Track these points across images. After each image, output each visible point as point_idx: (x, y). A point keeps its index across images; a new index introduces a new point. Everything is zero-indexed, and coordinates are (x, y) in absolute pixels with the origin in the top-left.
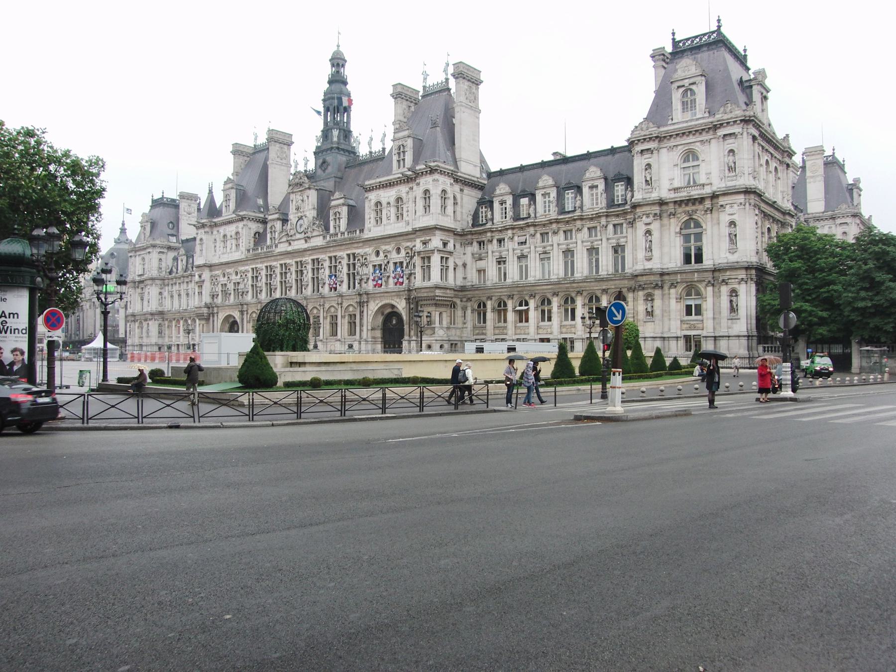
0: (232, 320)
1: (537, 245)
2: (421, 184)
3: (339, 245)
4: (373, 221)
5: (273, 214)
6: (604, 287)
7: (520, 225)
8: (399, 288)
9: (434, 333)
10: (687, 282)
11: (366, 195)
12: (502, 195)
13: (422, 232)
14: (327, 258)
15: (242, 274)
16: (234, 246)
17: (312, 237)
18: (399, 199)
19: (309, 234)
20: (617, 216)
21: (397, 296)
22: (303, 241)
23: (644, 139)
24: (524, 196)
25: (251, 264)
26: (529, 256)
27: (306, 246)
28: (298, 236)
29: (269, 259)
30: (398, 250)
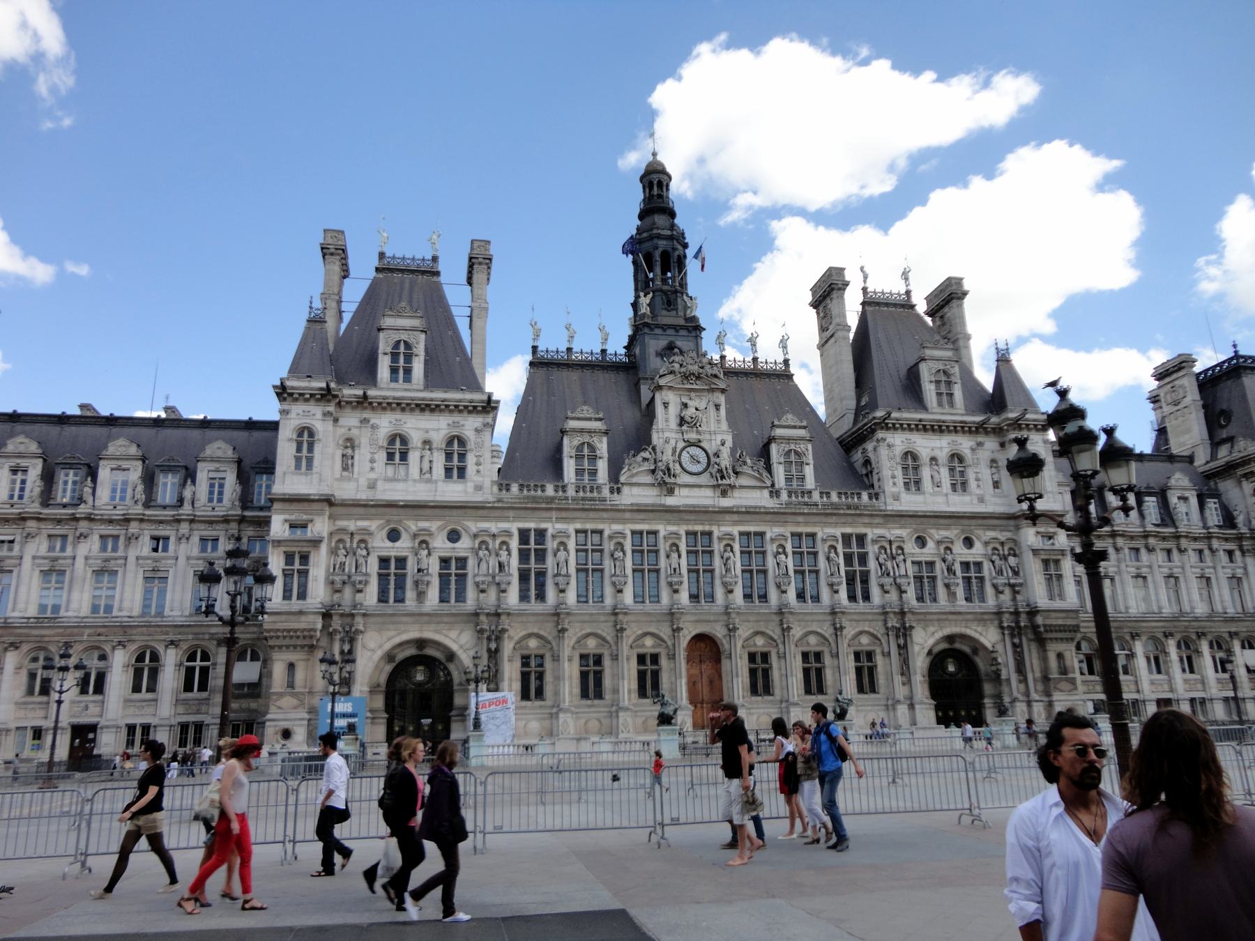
0: (411, 651)
3: (821, 514)
4: (900, 480)
5: (590, 419)
6: (1233, 630)
8: (980, 607)
9: (1076, 688)
14: (789, 535)
15: (490, 541)
16: (439, 470)
17: (742, 487)
18: (956, 457)
19: (732, 480)
20: (1226, 540)
21: (980, 620)
22: (709, 492)
25: (515, 519)
26: (1117, 578)
27: (726, 502)
28: (685, 479)
29: (592, 514)
30: (969, 542)
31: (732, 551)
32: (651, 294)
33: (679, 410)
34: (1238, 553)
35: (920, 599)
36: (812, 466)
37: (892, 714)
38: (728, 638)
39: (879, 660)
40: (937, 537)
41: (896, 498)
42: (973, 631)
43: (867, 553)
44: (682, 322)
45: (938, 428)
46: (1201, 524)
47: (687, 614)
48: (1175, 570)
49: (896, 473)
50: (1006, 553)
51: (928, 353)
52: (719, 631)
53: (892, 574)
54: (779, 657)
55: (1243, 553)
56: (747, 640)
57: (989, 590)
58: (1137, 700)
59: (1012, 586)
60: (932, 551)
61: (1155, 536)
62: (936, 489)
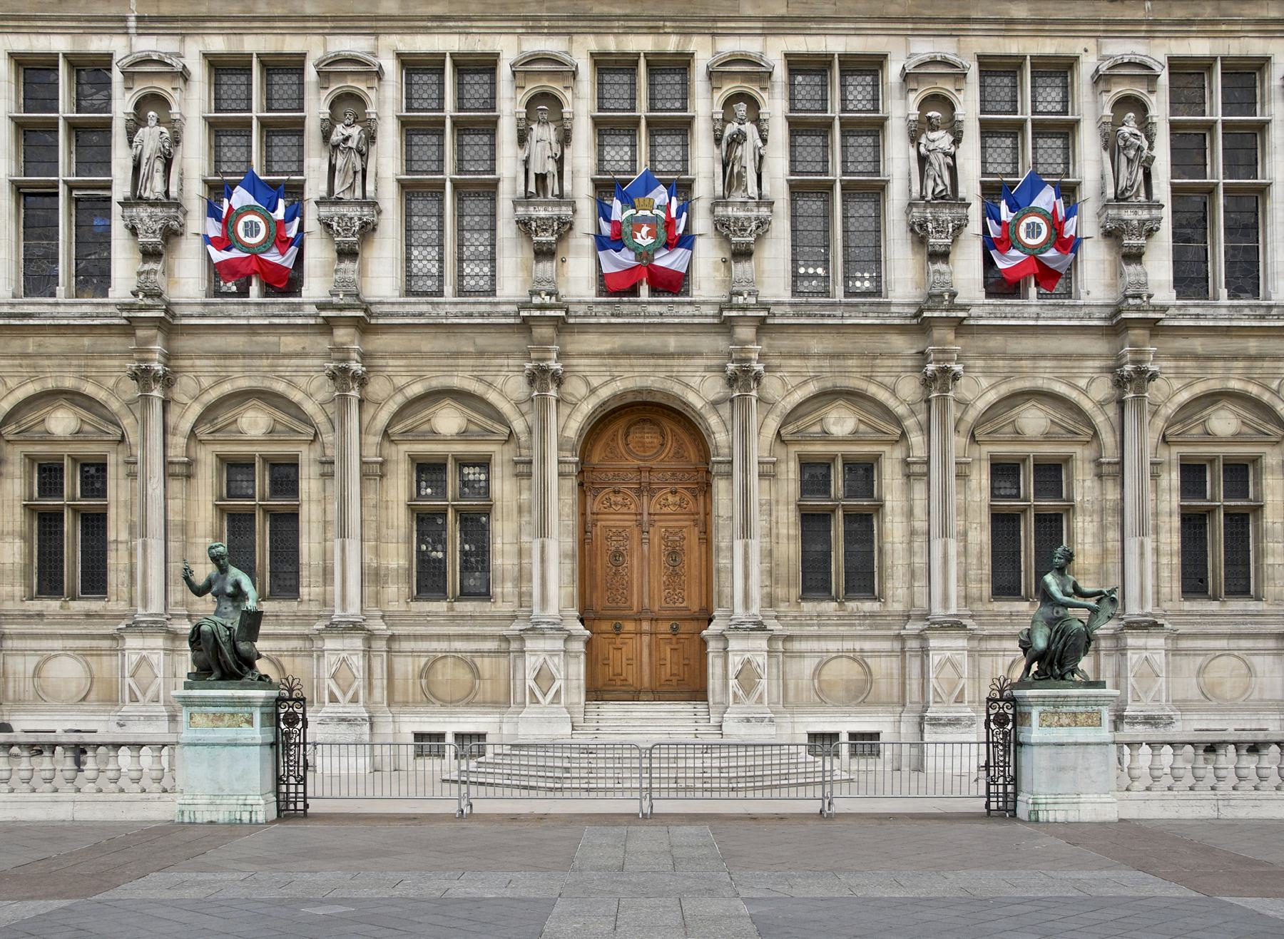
38: (725, 410)
54: (908, 476)
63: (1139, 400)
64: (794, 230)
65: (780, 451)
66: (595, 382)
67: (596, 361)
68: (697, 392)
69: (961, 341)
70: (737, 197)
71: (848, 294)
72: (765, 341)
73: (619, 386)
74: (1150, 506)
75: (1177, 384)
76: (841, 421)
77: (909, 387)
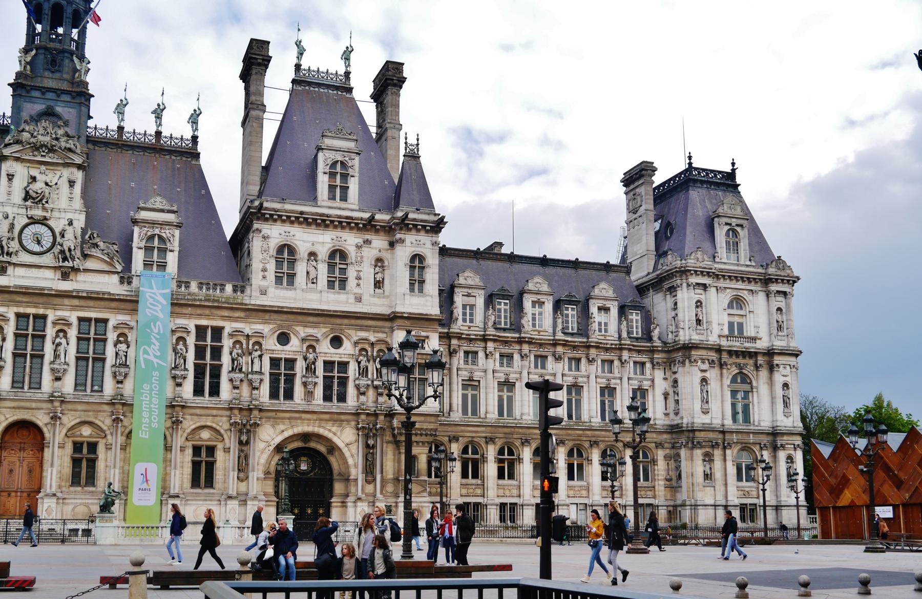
1: (531, 370)
2: (408, 242)
7: (508, 337)
8: (338, 407)
10: (742, 443)
11: (256, 225)
12: (470, 287)
13: (411, 321)
17: (86, 270)
18: (338, 255)
19: (77, 263)
20: (639, 352)
21: (335, 421)
22: (49, 274)
23: (702, 272)
24: (504, 297)
28: (25, 258)
30: (336, 342)
31: (65, 337)
32: (34, 52)
33: (26, 184)
34: (648, 365)
35: (274, 395)
36: (176, 253)
37: (223, 509)
38: (49, 426)
39: (220, 455)
40: (303, 335)
41: (264, 292)
42: (327, 430)
43: (222, 346)
44: (65, 86)
45: (323, 222)
46: (616, 335)
47: (5, 399)
48: (580, 379)
49: (268, 266)
50: (375, 354)
51: (328, 142)
52: (41, 419)
53: (244, 370)
54: (107, 448)
55: (653, 365)
56: (69, 430)
57: (351, 391)
58: (513, 505)
59: (376, 388)
60: (294, 349)
61: (564, 345)
62: (310, 285)
63: (177, 428)
64: (76, 370)
65: (66, 440)
66: (7, 416)
67: (8, 410)
68: (40, 420)
69: (125, 408)
70: (58, 361)
71: (92, 391)
72: (64, 406)
73: (15, 418)
74: (178, 460)
75: (191, 423)
76: (86, 431)
77: (108, 421)
